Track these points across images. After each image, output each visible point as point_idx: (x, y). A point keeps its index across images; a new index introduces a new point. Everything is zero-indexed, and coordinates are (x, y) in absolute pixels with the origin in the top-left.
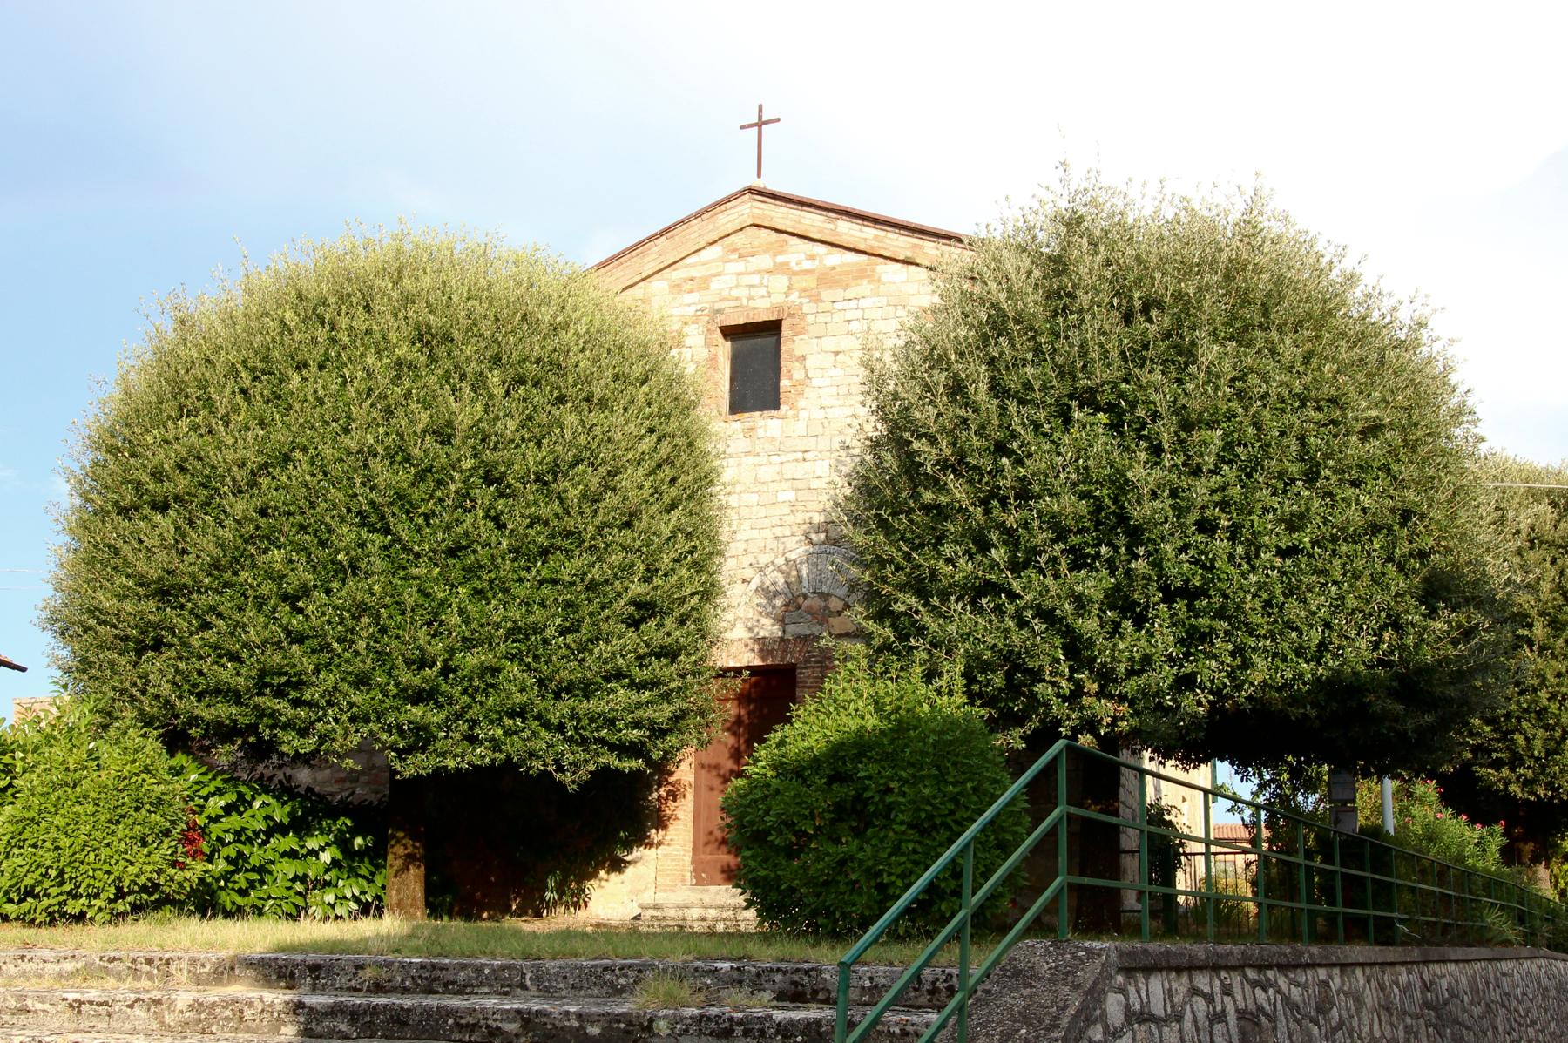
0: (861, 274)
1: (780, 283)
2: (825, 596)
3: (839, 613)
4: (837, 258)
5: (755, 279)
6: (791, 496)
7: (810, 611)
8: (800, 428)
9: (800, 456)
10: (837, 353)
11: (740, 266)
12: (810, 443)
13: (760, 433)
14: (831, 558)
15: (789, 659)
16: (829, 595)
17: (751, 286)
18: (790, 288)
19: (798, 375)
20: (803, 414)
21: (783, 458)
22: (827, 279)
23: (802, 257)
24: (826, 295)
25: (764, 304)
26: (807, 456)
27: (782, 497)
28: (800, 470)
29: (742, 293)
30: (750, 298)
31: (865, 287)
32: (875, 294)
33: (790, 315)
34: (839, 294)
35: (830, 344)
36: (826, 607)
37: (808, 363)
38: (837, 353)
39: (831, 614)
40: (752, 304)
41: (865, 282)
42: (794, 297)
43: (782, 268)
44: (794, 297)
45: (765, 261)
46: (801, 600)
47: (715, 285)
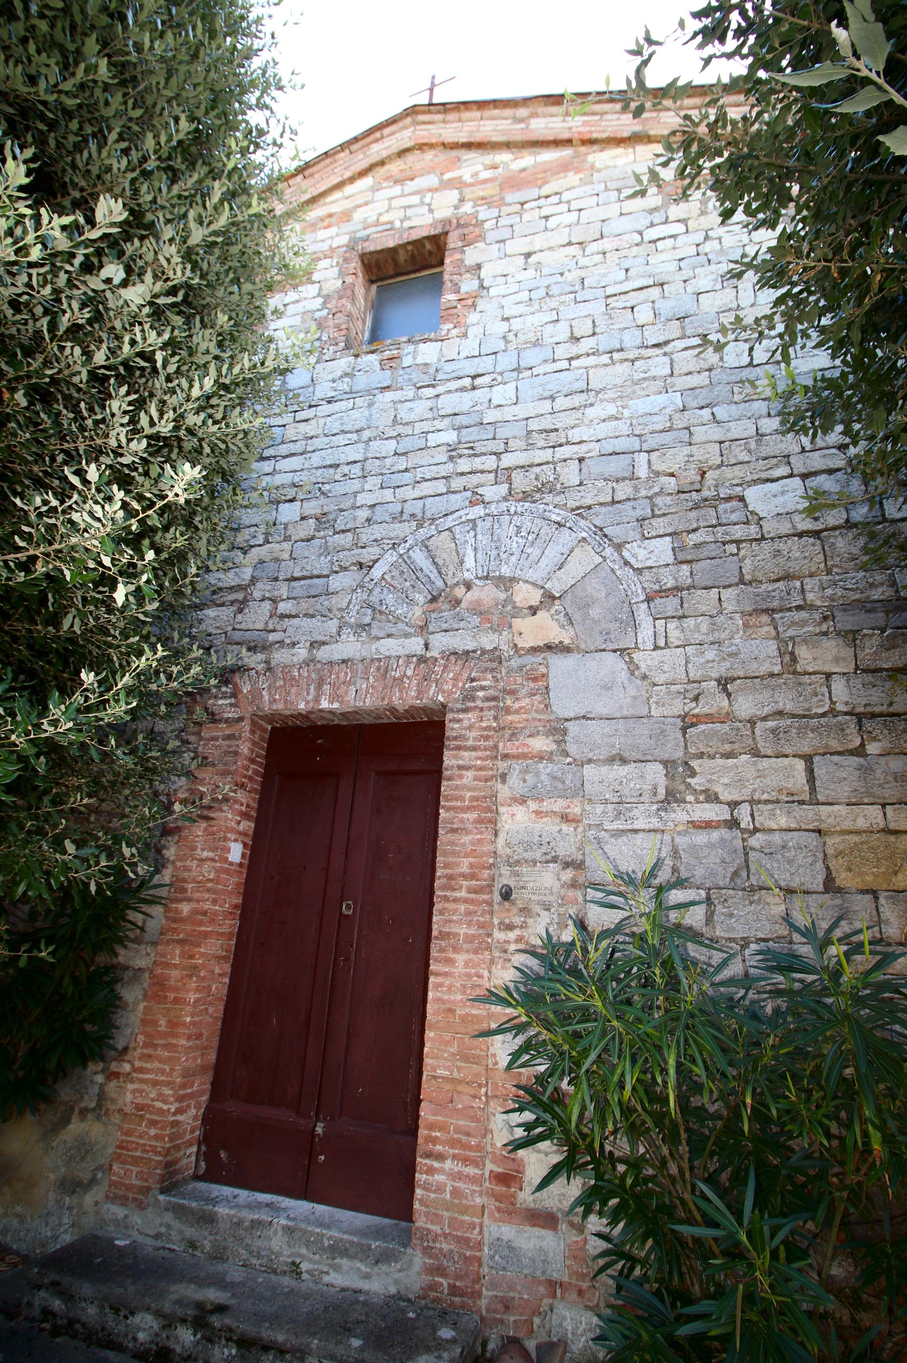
0: (565, 167)
1: (453, 196)
2: (507, 583)
3: (533, 610)
4: (527, 160)
5: (415, 199)
6: (450, 437)
7: (478, 610)
8: (470, 346)
9: (467, 382)
10: (528, 255)
11: (397, 190)
12: (485, 364)
13: (407, 361)
14: (517, 520)
15: (434, 695)
16: (513, 580)
17: (405, 208)
18: (462, 200)
19: (468, 285)
20: (471, 332)
21: (440, 389)
22: (513, 182)
23: (480, 167)
24: (510, 198)
25: (428, 219)
26: (478, 381)
27: (433, 439)
28: (465, 401)
29: (395, 216)
30: (407, 218)
31: (572, 178)
32: (584, 182)
33: (459, 226)
34: (534, 193)
35: (517, 246)
36: (508, 601)
37: (483, 274)
38: (528, 255)
39: (517, 612)
40: (407, 224)
41: (571, 174)
42: (467, 208)
43: (458, 184)
44: (467, 208)
45: (432, 180)
46: (460, 592)
47: (358, 216)
